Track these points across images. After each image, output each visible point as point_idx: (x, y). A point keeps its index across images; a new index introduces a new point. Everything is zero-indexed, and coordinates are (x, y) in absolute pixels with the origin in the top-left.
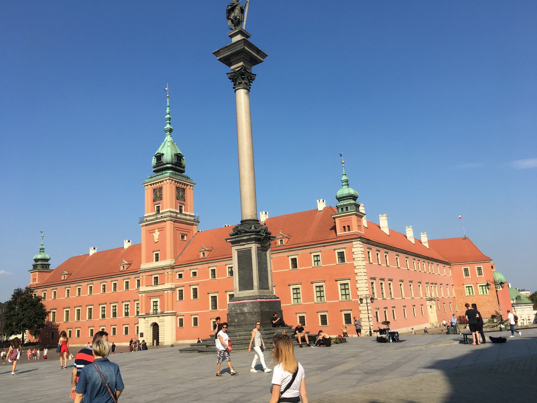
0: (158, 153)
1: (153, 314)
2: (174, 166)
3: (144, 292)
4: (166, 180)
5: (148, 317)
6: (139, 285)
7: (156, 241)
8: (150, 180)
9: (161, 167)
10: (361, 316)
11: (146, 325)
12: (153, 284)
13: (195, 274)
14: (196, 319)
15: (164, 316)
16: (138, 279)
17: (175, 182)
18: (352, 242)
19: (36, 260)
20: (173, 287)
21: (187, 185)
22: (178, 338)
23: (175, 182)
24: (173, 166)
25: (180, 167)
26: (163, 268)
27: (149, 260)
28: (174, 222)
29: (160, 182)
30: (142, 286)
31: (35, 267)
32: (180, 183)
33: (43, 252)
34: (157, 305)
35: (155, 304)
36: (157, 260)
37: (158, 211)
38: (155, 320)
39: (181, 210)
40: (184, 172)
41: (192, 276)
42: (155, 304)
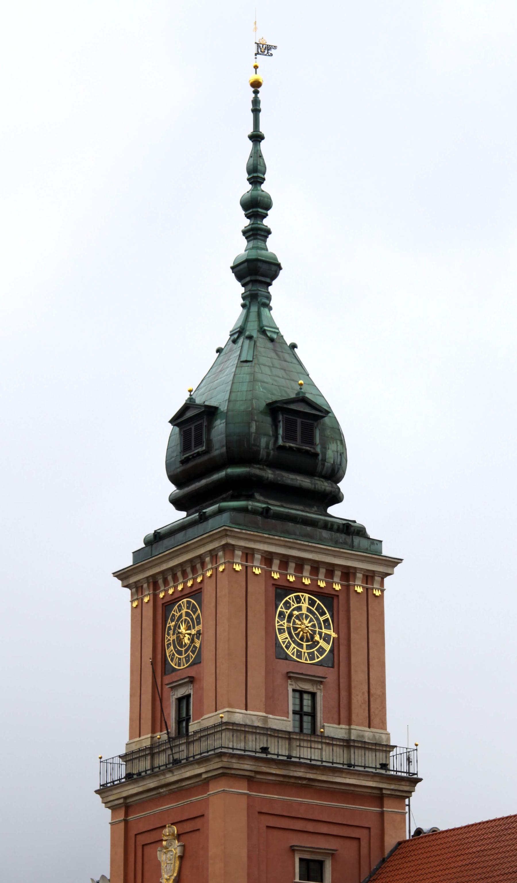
17: (268, 559)
21: (348, 574)
23: (268, 559)
37: (183, 720)
40: (336, 498)
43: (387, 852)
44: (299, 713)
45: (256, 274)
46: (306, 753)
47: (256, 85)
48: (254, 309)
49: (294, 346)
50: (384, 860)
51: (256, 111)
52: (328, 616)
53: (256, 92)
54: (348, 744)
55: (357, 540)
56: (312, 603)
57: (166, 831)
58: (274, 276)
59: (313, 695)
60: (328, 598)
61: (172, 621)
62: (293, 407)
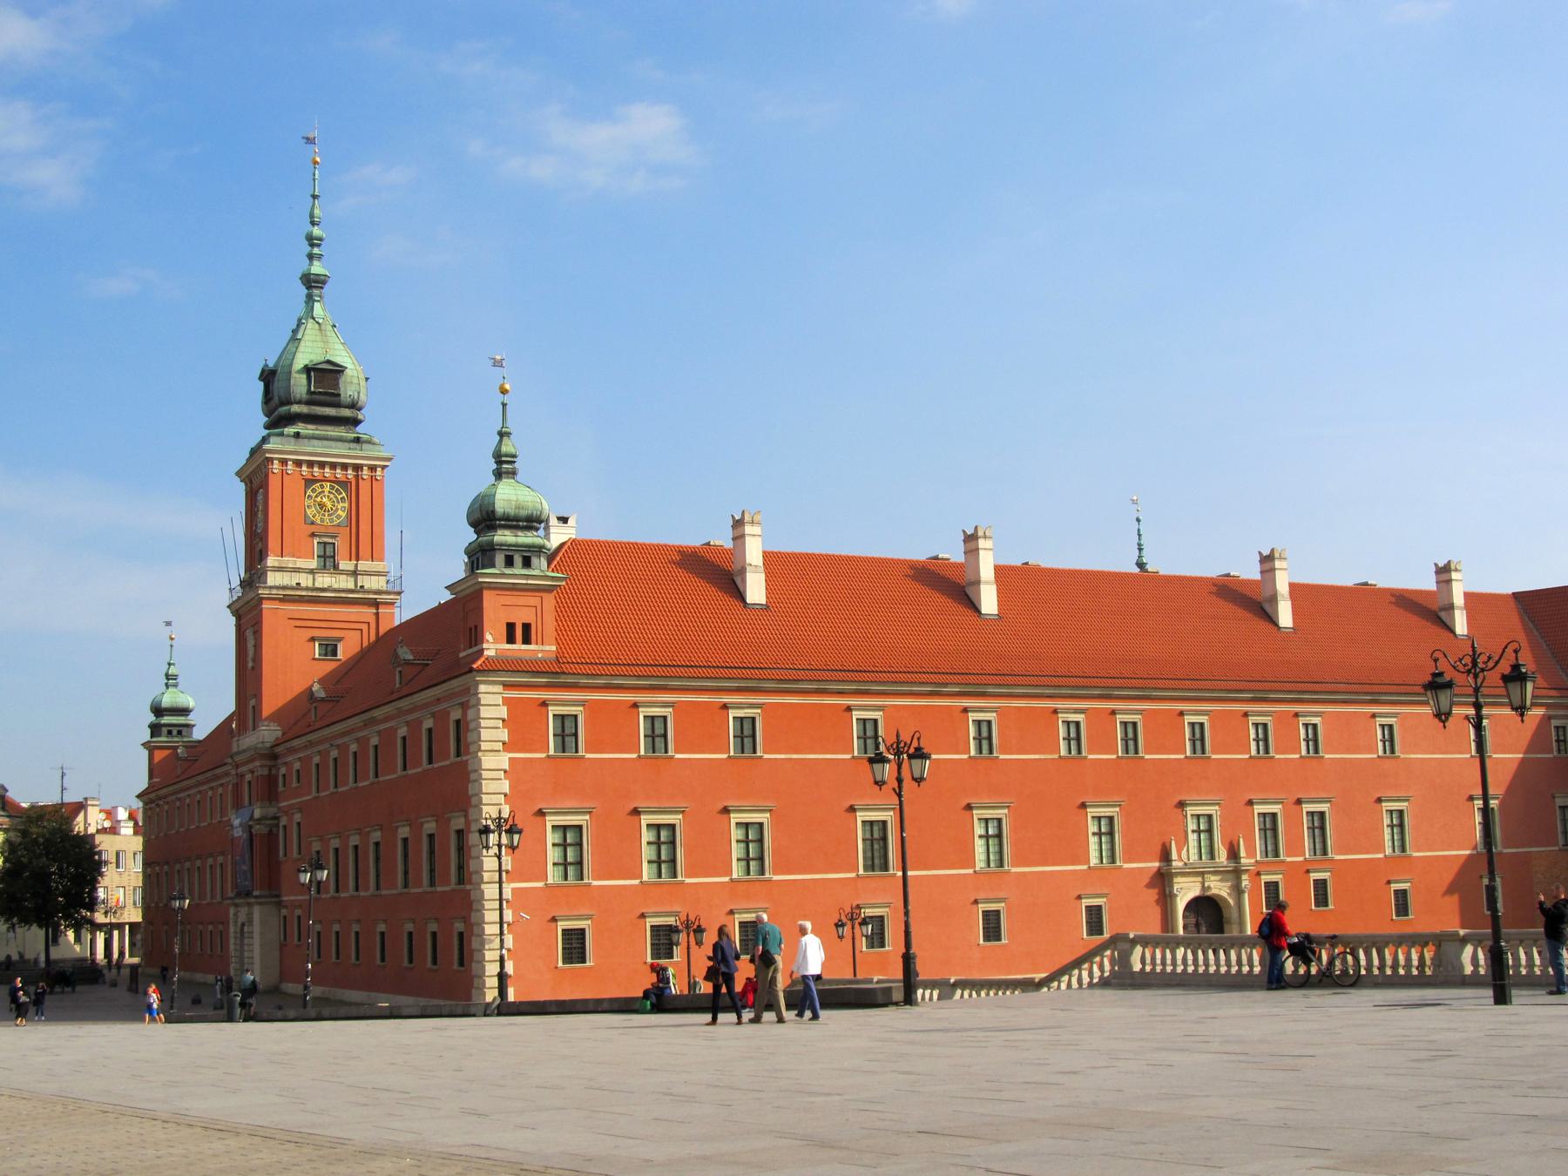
0: (263, 371)
5: (236, 905)
10: (475, 945)
17: (298, 463)
18: (468, 690)
19: (158, 711)
20: (272, 811)
21: (357, 468)
22: (284, 975)
25: (338, 405)
27: (243, 727)
28: (281, 600)
31: (155, 729)
32: (322, 465)
33: (175, 686)
40: (356, 422)
41: (294, 784)
44: (323, 556)
46: (324, 580)
58: (324, 282)
60: (344, 484)
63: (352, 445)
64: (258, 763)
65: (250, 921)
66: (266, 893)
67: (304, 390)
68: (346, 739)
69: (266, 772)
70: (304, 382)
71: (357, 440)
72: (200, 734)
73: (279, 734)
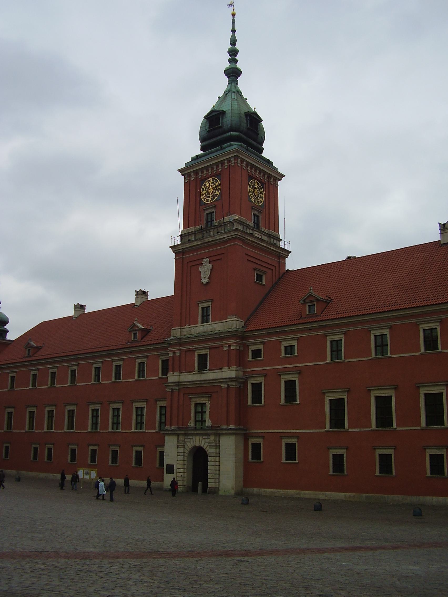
0: (212, 111)
1: (195, 429)
2: (245, 137)
3: (178, 384)
4: (229, 160)
5: (185, 435)
6: (165, 372)
7: (205, 281)
8: (196, 161)
9: (219, 138)
11: (181, 450)
12: (196, 368)
13: (289, 350)
14: (290, 448)
15: (219, 435)
16: (165, 358)
17: (248, 163)
21: (269, 176)
24: (241, 134)
25: (255, 140)
26: (220, 337)
29: (217, 164)
30: (173, 371)
32: (256, 168)
34: (203, 412)
35: (199, 409)
36: (205, 319)
37: (209, 221)
38: (198, 441)
39: (257, 224)
41: (283, 355)
42: (199, 409)
43: (281, 276)
45: (233, 74)
47: (233, 15)
48: (233, 85)
49: (247, 99)
50: (280, 279)
51: (233, 22)
52: (262, 190)
53: (233, 17)
54: (269, 236)
55: (271, 166)
56: (258, 184)
57: (205, 260)
59: (258, 217)
61: (204, 186)
62: (253, 115)
63: (266, 163)
64: (234, 341)
65: (218, 446)
66: (238, 427)
67: (245, 125)
68: (410, 321)
69: (238, 348)
70: (245, 121)
71: (269, 163)
72: (11, 336)
73: (243, 323)
